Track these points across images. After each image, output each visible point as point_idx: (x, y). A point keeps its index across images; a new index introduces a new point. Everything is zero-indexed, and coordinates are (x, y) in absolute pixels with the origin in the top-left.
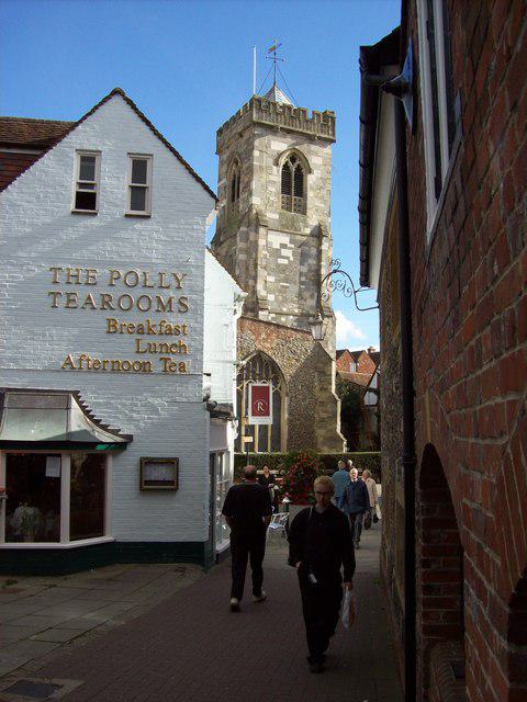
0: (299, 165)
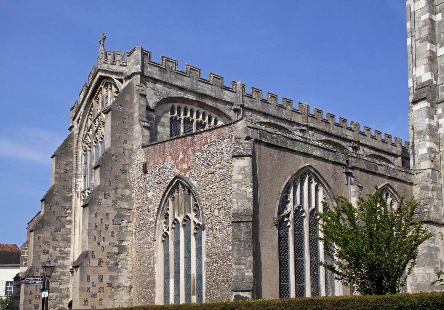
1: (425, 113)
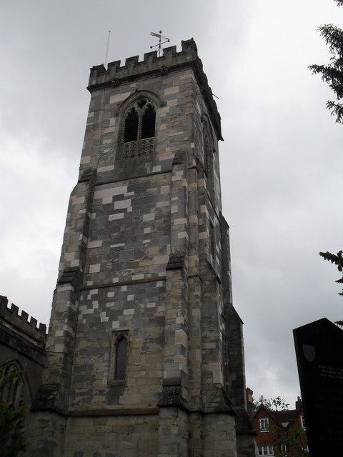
0: (149, 106)
1: (67, 296)
